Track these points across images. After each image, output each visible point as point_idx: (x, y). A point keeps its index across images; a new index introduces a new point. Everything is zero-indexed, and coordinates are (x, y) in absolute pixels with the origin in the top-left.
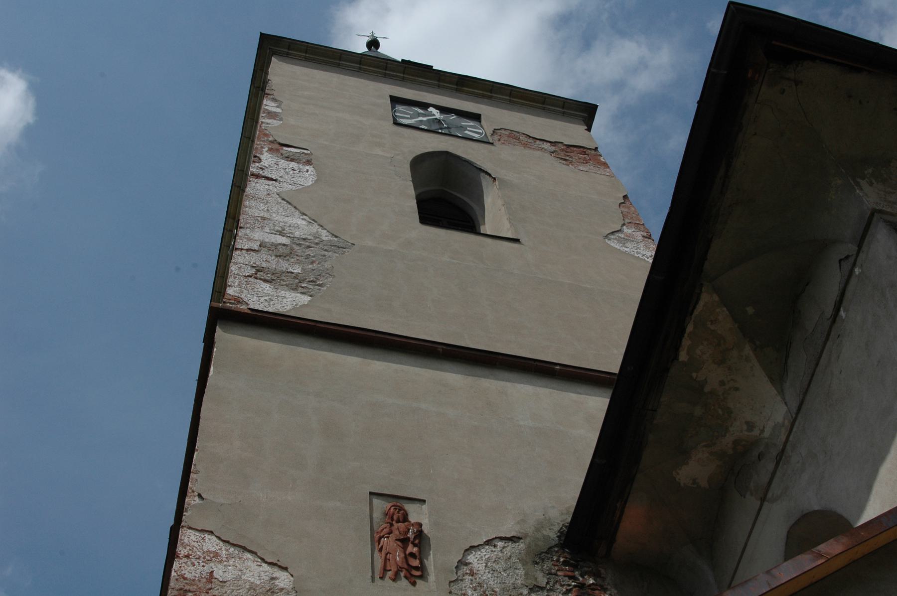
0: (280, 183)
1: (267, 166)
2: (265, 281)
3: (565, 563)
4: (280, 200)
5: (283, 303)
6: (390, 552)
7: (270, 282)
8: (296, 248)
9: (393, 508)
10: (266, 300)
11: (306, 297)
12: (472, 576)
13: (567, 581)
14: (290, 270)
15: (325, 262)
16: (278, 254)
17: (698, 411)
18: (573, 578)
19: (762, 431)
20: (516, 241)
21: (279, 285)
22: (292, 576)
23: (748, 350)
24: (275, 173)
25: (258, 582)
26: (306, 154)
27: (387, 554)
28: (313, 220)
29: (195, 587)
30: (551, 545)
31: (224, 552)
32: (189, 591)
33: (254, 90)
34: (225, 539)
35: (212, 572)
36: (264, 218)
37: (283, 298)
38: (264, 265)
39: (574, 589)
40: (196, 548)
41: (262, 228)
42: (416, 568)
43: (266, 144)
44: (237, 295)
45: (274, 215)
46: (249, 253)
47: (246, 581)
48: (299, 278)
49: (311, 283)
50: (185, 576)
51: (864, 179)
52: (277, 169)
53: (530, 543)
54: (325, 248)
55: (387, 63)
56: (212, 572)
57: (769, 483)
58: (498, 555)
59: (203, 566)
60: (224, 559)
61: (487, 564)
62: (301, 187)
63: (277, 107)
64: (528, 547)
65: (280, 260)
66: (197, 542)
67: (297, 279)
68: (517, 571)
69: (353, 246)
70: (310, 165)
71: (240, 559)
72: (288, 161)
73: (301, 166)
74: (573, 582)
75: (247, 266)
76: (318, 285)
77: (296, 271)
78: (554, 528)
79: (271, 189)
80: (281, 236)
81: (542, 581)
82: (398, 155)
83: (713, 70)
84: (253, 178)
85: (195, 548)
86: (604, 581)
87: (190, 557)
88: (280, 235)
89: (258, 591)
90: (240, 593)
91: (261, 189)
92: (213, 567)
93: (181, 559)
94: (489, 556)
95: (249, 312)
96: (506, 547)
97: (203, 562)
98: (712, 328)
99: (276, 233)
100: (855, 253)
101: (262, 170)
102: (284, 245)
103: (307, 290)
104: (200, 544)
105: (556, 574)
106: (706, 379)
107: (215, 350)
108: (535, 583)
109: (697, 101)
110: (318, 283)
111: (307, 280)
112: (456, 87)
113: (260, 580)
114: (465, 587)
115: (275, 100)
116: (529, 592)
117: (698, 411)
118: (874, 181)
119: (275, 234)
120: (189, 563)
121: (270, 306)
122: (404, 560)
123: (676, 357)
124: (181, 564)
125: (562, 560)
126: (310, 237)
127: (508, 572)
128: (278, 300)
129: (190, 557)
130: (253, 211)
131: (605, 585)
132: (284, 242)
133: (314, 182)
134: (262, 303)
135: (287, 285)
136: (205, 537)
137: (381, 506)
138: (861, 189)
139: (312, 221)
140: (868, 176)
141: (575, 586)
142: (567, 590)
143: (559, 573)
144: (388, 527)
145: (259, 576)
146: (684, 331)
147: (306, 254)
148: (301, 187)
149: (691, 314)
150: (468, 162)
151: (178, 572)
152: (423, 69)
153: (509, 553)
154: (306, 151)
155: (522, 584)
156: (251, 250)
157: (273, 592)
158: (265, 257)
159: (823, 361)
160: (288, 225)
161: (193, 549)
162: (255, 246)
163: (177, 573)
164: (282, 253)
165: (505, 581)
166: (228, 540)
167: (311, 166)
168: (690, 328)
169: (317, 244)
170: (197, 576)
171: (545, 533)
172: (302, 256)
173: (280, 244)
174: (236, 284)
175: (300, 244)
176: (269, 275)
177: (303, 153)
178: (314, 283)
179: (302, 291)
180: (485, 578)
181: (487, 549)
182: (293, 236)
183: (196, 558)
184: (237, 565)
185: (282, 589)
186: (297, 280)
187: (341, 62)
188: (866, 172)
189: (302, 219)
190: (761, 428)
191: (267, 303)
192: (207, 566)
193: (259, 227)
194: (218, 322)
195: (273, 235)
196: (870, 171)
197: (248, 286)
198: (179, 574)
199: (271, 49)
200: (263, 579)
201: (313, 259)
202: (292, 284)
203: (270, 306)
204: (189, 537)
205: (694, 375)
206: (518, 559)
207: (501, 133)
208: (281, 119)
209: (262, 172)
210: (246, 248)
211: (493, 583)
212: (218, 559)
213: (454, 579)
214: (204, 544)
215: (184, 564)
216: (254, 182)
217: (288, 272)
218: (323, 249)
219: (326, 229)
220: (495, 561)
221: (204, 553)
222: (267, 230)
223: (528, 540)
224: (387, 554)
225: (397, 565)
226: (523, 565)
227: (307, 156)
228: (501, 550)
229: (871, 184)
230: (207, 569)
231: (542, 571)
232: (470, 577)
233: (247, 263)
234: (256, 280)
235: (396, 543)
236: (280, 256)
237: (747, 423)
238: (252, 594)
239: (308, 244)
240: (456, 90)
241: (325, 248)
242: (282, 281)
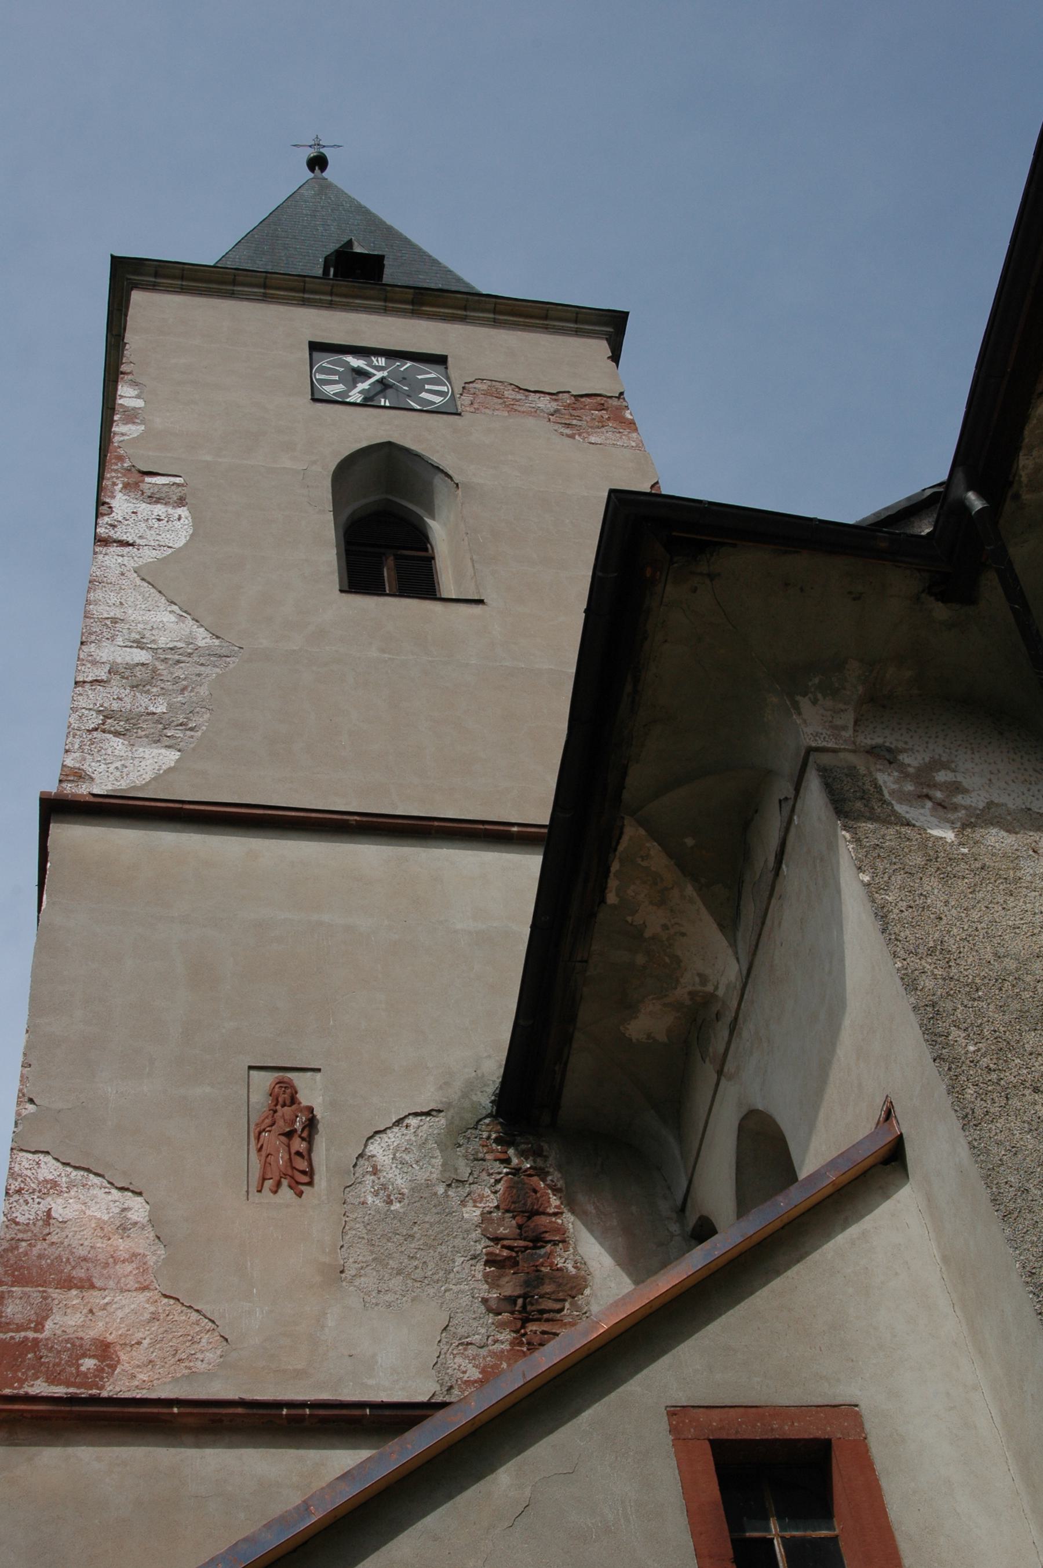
0: (138, 549)
1: (120, 519)
2: (117, 734)
3: (497, 1141)
4: (138, 581)
5: (142, 771)
6: (272, 1153)
7: (123, 735)
8: (161, 666)
9: (277, 1086)
10: (117, 768)
11: (173, 753)
12: (375, 1174)
13: (498, 1167)
14: (152, 709)
15: (201, 686)
16: (135, 684)
17: (640, 959)
18: (507, 1161)
19: (716, 988)
20: (480, 602)
21: (137, 737)
22: (147, 1203)
23: (690, 890)
24: (132, 531)
25: (106, 1218)
26: (178, 485)
27: (267, 1156)
28: (185, 612)
29: (29, 1234)
30: (480, 1117)
31: (64, 1179)
32: (23, 1240)
33: (113, 340)
34: (64, 1161)
35: (50, 1209)
36: (115, 620)
37: (141, 760)
38: (115, 706)
39: (505, 1179)
40: (30, 1177)
41: (112, 638)
42: (304, 1172)
43: (119, 475)
44: (77, 765)
45: (130, 612)
46: (93, 687)
47: (91, 1218)
48: (163, 721)
49: (180, 728)
50: (17, 1220)
51: (804, 695)
52: (135, 522)
53: (453, 1117)
54: (201, 662)
55: (304, 282)
56: (50, 1209)
57: (724, 1054)
58: (410, 1140)
59: (39, 1203)
60: (65, 1189)
61: (394, 1155)
62: (170, 551)
63: (138, 397)
64: (450, 1124)
65: (137, 694)
66: (30, 1169)
67: (161, 723)
68: (433, 1161)
69: (241, 650)
70: (184, 506)
71: (83, 1186)
72: (150, 503)
73: (170, 510)
74: (505, 1167)
75: (92, 712)
76: (191, 729)
77: (159, 710)
78: (488, 1090)
79: (125, 563)
80: (139, 650)
81: (464, 1172)
82: (314, 462)
83: (599, 574)
84: (99, 546)
85: (28, 1179)
86: (545, 1161)
87: (23, 1192)
88: (137, 647)
89: (106, 1230)
90: (84, 1235)
91: (112, 566)
92: (51, 1203)
93: (12, 1196)
94: (398, 1142)
95: (92, 799)
96: (422, 1126)
97: (38, 1197)
98: (644, 864)
99: (132, 644)
100: (793, 797)
101: (113, 529)
102: (143, 664)
103: (174, 741)
104: (34, 1171)
105: (484, 1160)
106: (644, 923)
107: (49, 865)
108: (455, 1177)
109: (583, 610)
110: (190, 726)
111: (175, 723)
112: (411, 307)
113: (109, 1213)
114: (364, 1193)
115: (134, 384)
116: (445, 1190)
117: (640, 959)
118: (820, 696)
119: (131, 647)
120: (21, 1201)
121: (123, 778)
122: (289, 1164)
123: (603, 900)
124: (12, 1203)
125: (494, 1136)
126: (180, 645)
127: (421, 1164)
128: (134, 765)
129: (23, 1192)
130: (100, 608)
131: (547, 1167)
132: (143, 660)
133: (188, 538)
134: (112, 773)
135: (147, 736)
136: (40, 1160)
137: (264, 1081)
138: (800, 714)
139: (184, 614)
140: (813, 690)
141: (507, 1174)
142: (496, 1180)
143: (488, 1157)
144: (270, 1116)
145: (107, 1209)
146: (608, 871)
147: (174, 676)
148: (170, 551)
149: (615, 850)
150: (420, 456)
151: (9, 1215)
152: (361, 285)
153: (425, 1135)
154: (178, 480)
155: (437, 1179)
156: (96, 681)
157: (125, 1228)
158: (116, 690)
159: (768, 922)
160: (149, 627)
161: (25, 1179)
162: (102, 674)
163: (7, 1218)
164: (141, 680)
165: (417, 1178)
166: (68, 1162)
167: (185, 508)
168: (615, 866)
169: (190, 655)
170: (32, 1218)
171: (474, 1098)
172: (168, 681)
173: (137, 664)
174: (77, 746)
175: (166, 659)
176: (122, 723)
177: (174, 484)
178: (184, 727)
179: (167, 744)
180: (390, 1176)
181: (396, 1133)
182: (156, 647)
183: (30, 1193)
184: (81, 1196)
185: (136, 1223)
186: (161, 726)
187: (235, 288)
188: (810, 684)
189: (170, 611)
190: (716, 983)
191: (118, 774)
192: (43, 1202)
193: (108, 639)
194: (52, 817)
195: (128, 649)
196: (816, 680)
197: (93, 746)
198: (9, 1218)
199: (130, 279)
200: (112, 1212)
201: (184, 682)
202: (153, 734)
203: (123, 778)
204: (20, 1164)
205: (629, 919)
206: (436, 1143)
207: (475, 388)
208: (143, 422)
209: (113, 532)
210: (90, 679)
211: (401, 1182)
212: (57, 1190)
213: (350, 1184)
214: (39, 1170)
215: (15, 1204)
216: (101, 553)
217: (148, 714)
218: (198, 663)
219: (202, 626)
220: (406, 1149)
221: (39, 1183)
222: (119, 641)
223: (450, 1114)
224: (267, 1156)
225: (280, 1171)
226: (441, 1151)
227: (180, 488)
228: (415, 1132)
229: (814, 702)
230: (43, 1207)
231: (466, 1157)
232: (372, 1177)
233: (91, 706)
234: (104, 735)
235: (279, 1139)
236: (137, 686)
237: (700, 975)
238: (99, 1235)
239: (177, 657)
240: (412, 313)
241: (202, 660)
242: (139, 731)
